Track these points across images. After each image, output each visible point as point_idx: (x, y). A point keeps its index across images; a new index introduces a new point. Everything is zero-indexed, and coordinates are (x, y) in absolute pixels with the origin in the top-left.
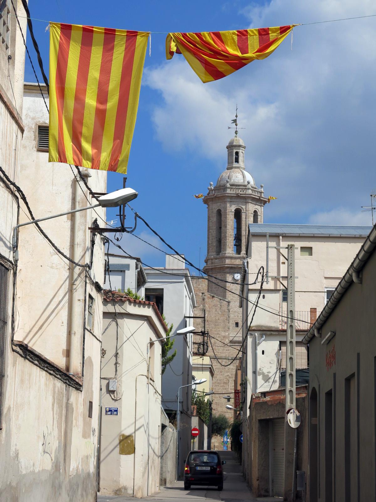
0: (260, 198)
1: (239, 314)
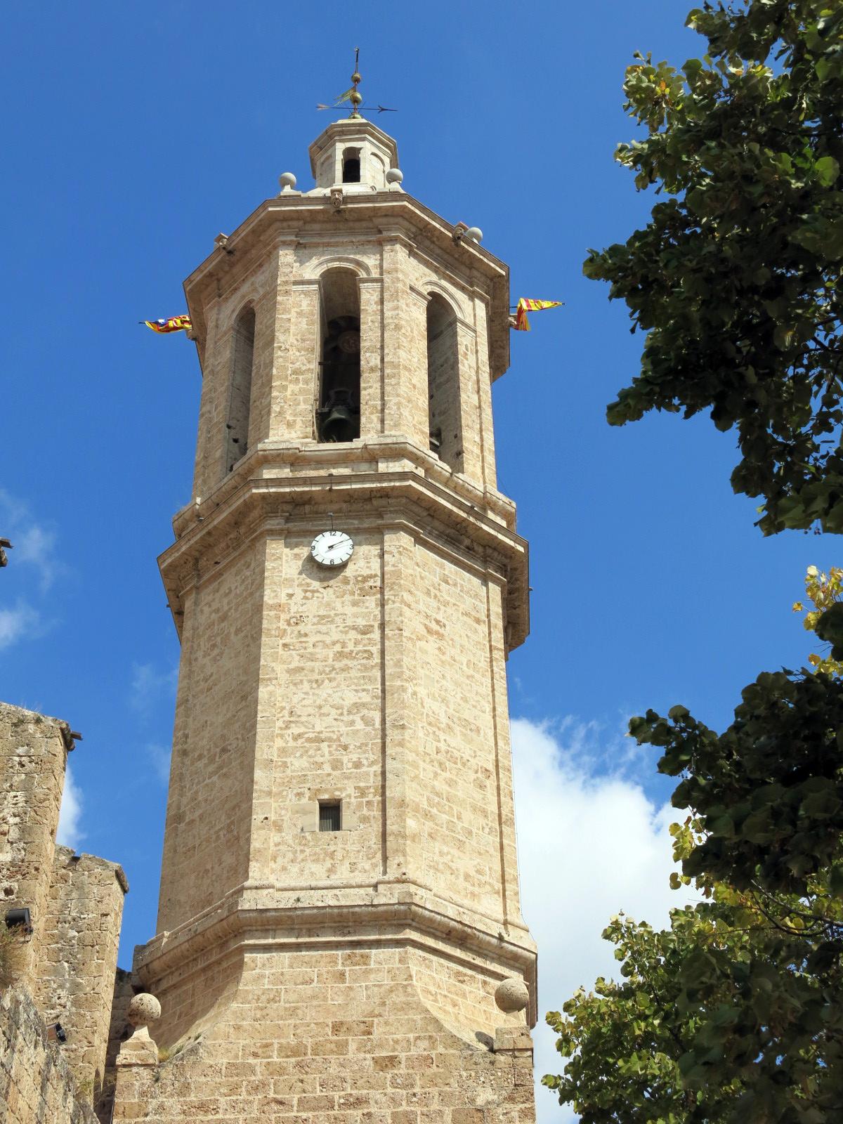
0: (457, 239)
1: (345, 748)
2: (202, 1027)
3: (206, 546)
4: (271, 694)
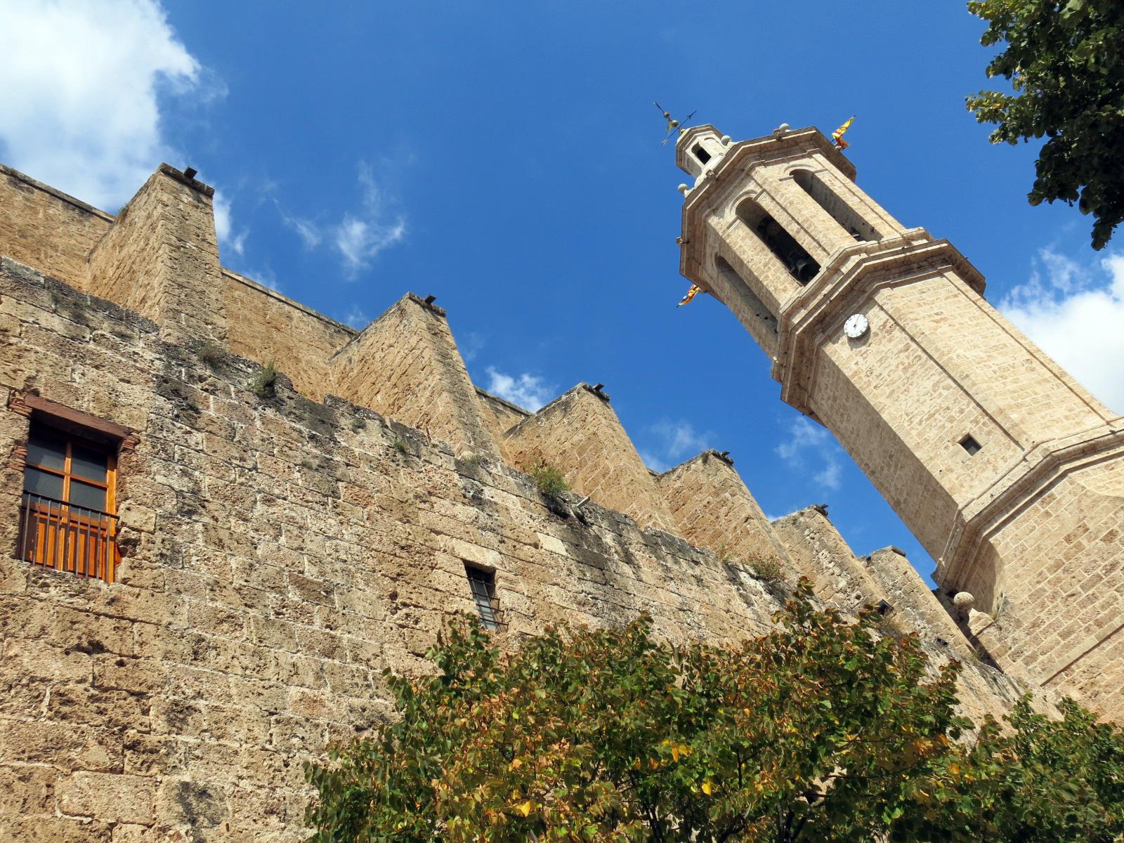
0: (779, 139)
1: (948, 408)
2: (999, 589)
3: (797, 375)
4: (889, 414)
